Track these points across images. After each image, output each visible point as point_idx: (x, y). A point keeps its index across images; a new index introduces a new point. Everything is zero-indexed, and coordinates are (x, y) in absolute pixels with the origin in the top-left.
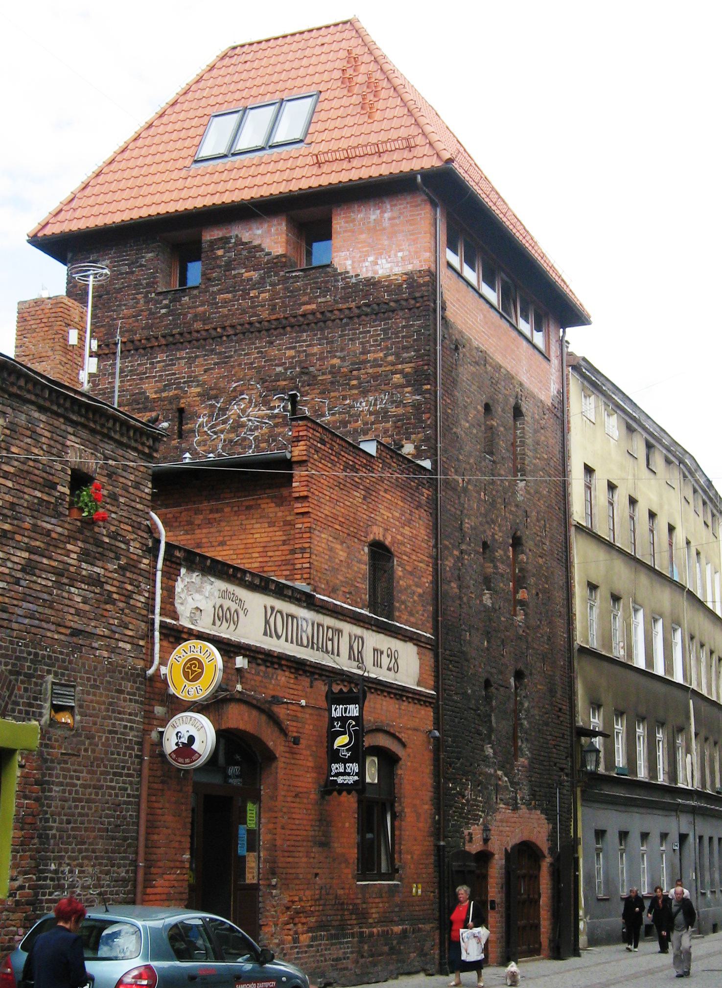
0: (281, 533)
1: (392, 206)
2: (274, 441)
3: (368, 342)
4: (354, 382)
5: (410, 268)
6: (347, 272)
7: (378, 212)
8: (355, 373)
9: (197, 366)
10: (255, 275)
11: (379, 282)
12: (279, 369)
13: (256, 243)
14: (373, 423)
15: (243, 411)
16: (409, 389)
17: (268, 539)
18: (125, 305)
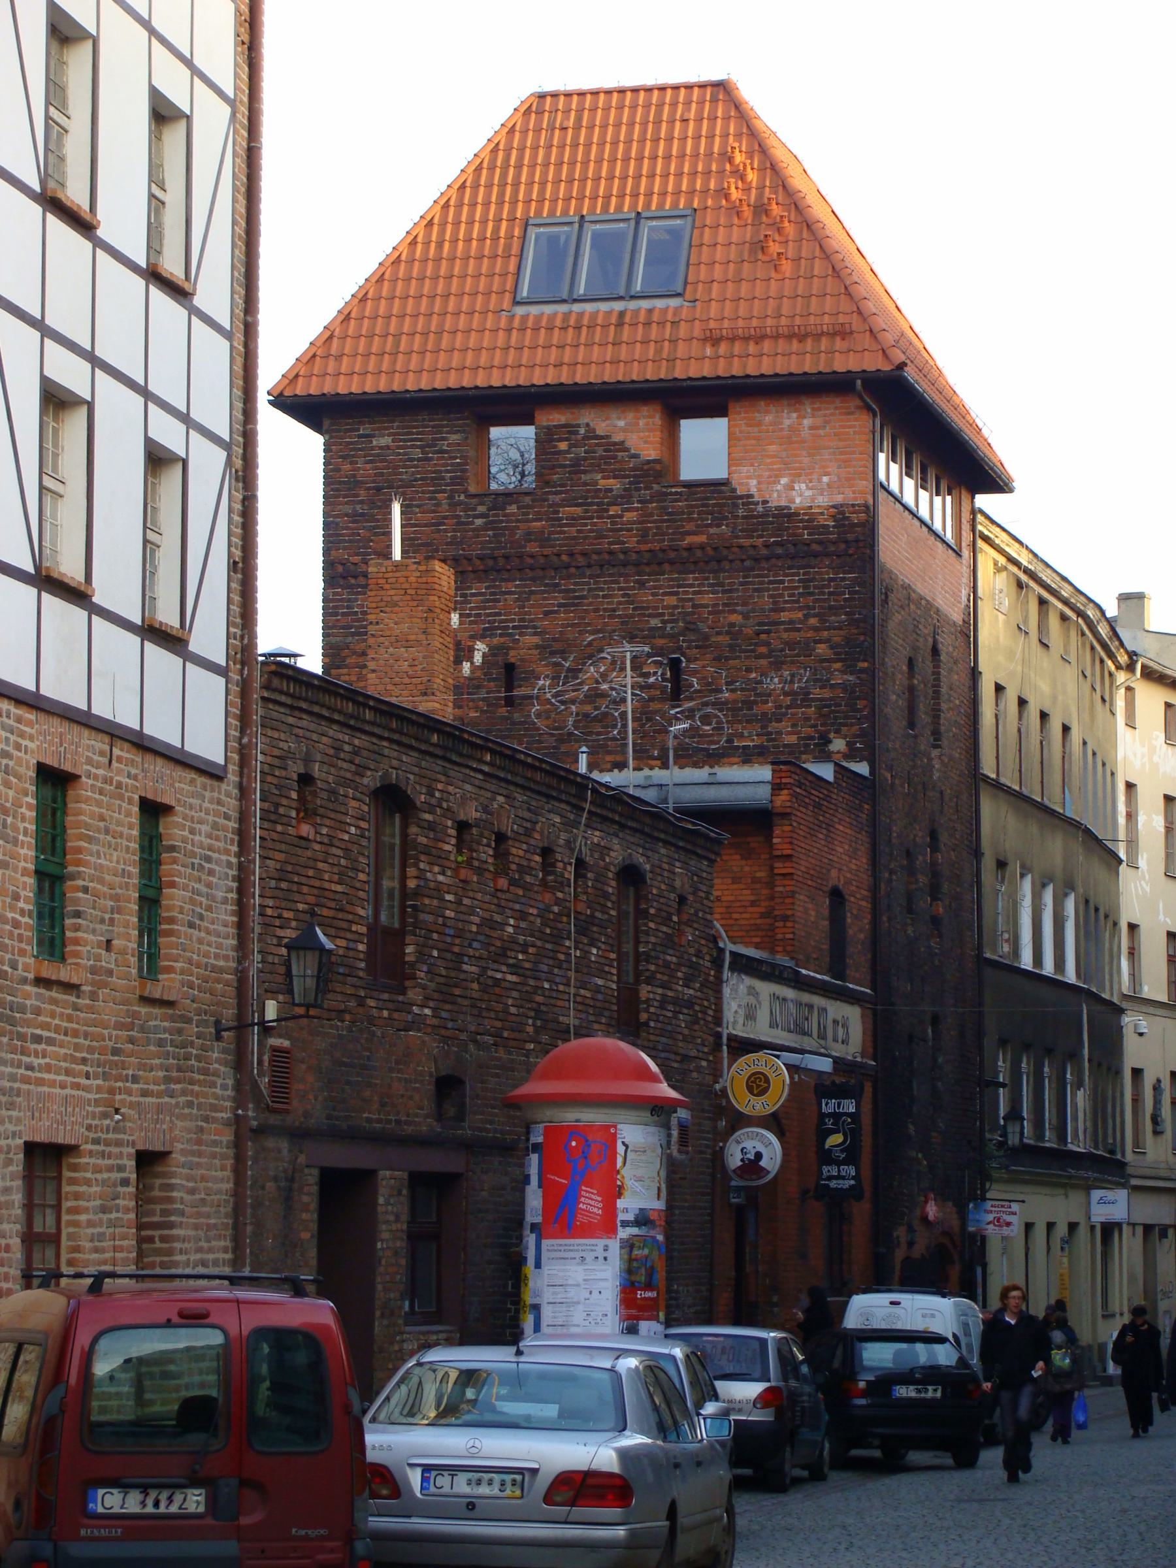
0: (748, 892)
1: (813, 409)
2: (648, 719)
3: (781, 595)
4: (763, 650)
5: (839, 499)
6: (751, 496)
7: (795, 415)
8: (763, 636)
9: (533, 606)
10: (615, 485)
11: (797, 514)
12: (655, 622)
13: (617, 438)
14: (788, 707)
15: (604, 676)
16: (838, 665)
17: (732, 898)
18: (418, 506)
